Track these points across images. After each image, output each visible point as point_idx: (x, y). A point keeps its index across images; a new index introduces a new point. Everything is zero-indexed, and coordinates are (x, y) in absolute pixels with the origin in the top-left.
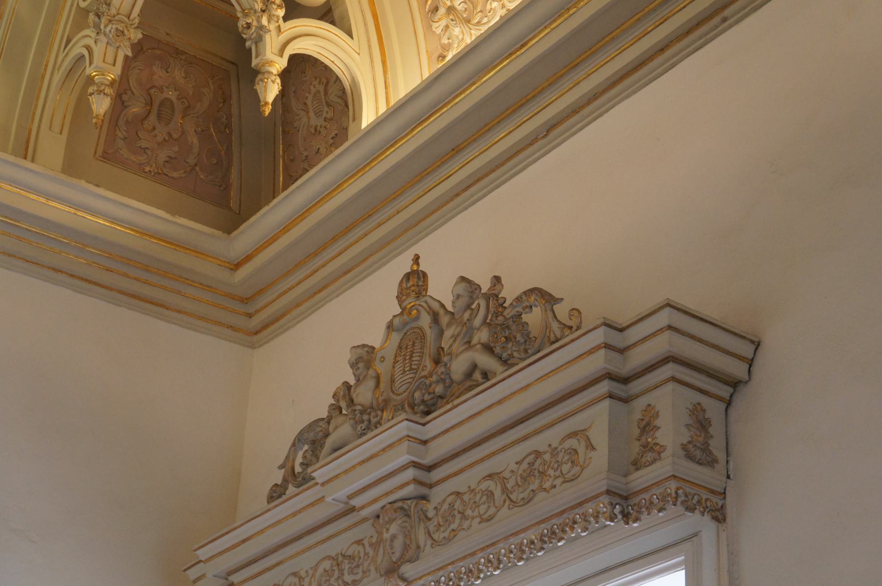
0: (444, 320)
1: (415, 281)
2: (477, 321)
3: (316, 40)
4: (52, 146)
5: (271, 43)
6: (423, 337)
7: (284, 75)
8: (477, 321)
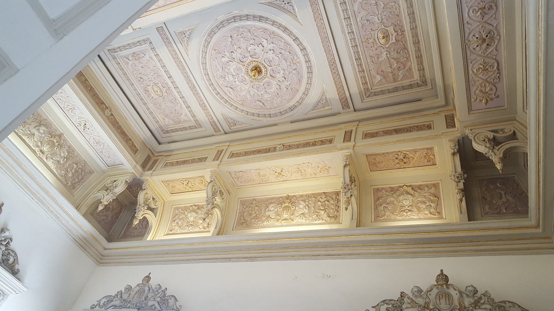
0: (151, 291)
1: (148, 278)
2: (158, 295)
3: (150, 216)
4: (84, 209)
5: (141, 213)
6: (144, 291)
7: (140, 220)
8: (158, 295)
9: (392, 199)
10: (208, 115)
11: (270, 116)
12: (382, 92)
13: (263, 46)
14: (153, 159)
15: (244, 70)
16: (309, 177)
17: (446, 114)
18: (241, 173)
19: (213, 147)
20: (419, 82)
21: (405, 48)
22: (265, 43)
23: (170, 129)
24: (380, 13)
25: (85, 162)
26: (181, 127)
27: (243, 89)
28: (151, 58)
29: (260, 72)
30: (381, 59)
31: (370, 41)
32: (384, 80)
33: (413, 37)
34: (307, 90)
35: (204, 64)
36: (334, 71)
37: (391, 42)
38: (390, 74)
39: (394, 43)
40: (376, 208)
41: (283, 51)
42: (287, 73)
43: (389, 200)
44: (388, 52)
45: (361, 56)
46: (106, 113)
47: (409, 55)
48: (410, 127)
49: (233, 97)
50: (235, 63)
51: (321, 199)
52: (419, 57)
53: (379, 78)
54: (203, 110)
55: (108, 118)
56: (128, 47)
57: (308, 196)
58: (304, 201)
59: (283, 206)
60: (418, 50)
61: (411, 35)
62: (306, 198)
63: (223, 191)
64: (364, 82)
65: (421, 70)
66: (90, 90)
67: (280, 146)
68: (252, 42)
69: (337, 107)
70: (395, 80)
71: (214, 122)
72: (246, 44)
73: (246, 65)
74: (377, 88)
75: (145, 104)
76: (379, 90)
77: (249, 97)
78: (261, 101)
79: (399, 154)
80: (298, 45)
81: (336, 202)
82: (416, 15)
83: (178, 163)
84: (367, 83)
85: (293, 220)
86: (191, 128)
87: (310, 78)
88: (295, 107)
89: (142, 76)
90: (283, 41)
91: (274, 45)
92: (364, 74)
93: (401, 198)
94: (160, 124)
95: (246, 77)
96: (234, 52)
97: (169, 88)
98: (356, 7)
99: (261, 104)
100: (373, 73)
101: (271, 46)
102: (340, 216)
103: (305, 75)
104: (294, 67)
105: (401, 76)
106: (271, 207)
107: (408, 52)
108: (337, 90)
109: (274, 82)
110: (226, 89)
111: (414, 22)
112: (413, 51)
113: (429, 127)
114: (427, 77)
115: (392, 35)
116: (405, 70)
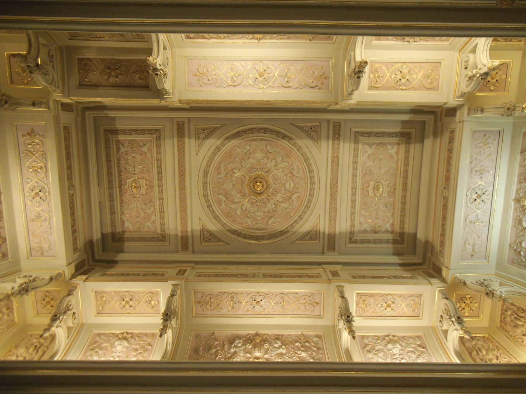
10: (336, 150)
13: (242, 209)
15: (271, 190)
18: (313, 85)
20: (111, 136)
22: (239, 212)
23: (398, 138)
25: (521, 153)
26: (381, 138)
27: (281, 170)
28: (361, 224)
30: (140, 167)
35: (307, 207)
41: (224, 199)
46: (447, 195)
50: (276, 200)
54: (338, 157)
55: (448, 189)
60: (109, 168)
61: (114, 183)
75: (405, 178)
76: (146, 135)
77: (279, 159)
86: (370, 134)
87: (208, 166)
90: (222, 207)
94: (406, 148)
95: (271, 181)
96: (271, 210)
98: (153, 217)
99: (269, 148)
101: (233, 206)
103: (212, 169)
104: (221, 180)
108: (184, 147)
112: (113, 168)
115: (128, 186)
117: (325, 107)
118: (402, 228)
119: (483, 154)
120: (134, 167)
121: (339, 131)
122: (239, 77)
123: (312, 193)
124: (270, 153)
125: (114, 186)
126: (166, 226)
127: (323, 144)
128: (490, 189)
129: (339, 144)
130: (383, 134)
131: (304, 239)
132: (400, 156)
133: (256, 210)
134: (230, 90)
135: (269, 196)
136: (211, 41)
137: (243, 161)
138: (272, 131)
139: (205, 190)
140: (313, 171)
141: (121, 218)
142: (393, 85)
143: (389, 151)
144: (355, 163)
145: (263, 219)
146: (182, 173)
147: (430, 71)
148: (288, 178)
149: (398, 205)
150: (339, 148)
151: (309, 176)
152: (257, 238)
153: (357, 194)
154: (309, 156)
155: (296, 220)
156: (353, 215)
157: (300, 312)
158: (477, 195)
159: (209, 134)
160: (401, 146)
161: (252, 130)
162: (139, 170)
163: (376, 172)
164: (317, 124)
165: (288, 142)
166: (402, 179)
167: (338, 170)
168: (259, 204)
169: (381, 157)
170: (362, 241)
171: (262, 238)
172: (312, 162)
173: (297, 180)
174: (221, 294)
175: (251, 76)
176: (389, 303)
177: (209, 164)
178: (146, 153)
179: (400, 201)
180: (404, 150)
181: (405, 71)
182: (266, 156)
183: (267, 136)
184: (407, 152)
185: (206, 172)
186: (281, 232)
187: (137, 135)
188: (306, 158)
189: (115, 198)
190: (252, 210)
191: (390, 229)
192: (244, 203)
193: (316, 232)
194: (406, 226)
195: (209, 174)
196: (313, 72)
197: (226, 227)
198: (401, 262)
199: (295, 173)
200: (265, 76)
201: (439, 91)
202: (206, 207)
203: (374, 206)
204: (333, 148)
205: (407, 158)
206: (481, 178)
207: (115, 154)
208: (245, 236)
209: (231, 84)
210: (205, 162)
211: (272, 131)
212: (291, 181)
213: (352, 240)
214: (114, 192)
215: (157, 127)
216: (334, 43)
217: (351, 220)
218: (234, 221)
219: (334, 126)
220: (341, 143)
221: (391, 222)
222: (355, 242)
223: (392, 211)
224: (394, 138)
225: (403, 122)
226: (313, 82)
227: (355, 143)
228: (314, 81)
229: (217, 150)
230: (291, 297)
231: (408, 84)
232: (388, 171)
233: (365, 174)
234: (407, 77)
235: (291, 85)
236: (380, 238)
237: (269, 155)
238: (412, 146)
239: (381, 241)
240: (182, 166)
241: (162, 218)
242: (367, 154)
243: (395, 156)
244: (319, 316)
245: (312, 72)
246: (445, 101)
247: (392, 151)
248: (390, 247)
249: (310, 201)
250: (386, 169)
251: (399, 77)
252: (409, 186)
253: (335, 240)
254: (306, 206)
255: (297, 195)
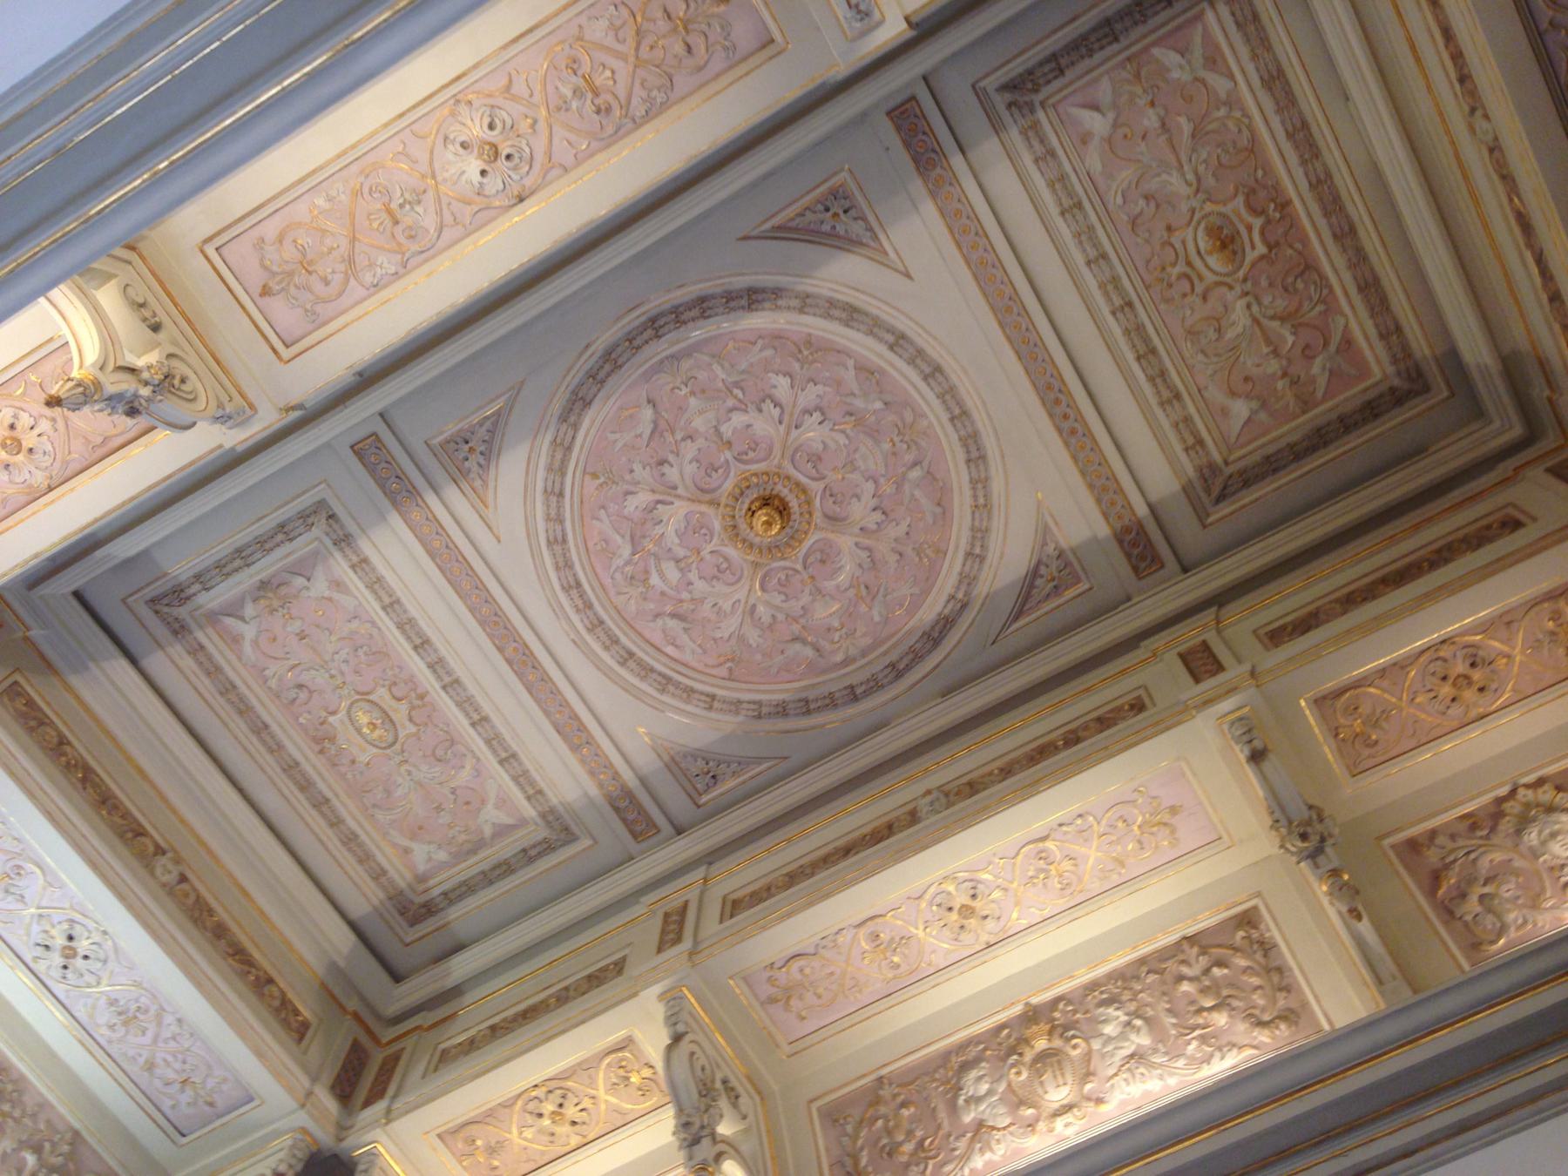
9: (1498, 856)
10: (597, 765)
11: (853, 695)
12: (1271, 465)
14: (377, 1057)
15: (717, 525)
16: (1097, 887)
17: (1549, 464)
18: (795, 966)
19: (638, 910)
20: (1396, 382)
21: (1308, 267)
23: (436, 892)
24: (1184, 159)
26: (485, 866)
27: (727, 606)
28: (338, 585)
29: (783, 510)
30: (1230, 334)
31: (1175, 271)
32: (1263, 416)
33: (1327, 214)
34: (980, 534)
35: (558, 542)
36: (1066, 425)
37: (1251, 256)
38: (1280, 384)
39: (1262, 257)
40: (1448, 912)
41: (859, 403)
42: (888, 488)
43: (1484, 864)
44: (1249, 298)
45: (1156, 341)
46: (158, 871)
47: (1331, 290)
48: (1439, 551)
49: (688, 657)
50: (677, 503)
51: (1185, 970)
52: (1370, 287)
53: (1241, 409)
54: (575, 749)
56: (238, 563)
57: (1126, 977)
58: (1111, 1001)
59: (1029, 1056)
60: (1359, 259)
62: (1118, 988)
63: (734, 1082)
64: (1191, 440)
65: (1391, 332)
66: (84, 780)
67: (928, 799)
68: (730, 403)
69: (1113, 569)
70: (1306, 404)
71: (628, 794)
72: (711, 415)
73: (723, 501)
74: (1249, 454)
76: (1256, 457)
77: (753, 636)
78: (804, 642)
79: (1445, 652)
80: (911, 362)
81: (1259, 956)
82: (1314, 129)
83: (495, 1032)
84: (1201, 442)
85: (1099, 1101)
86: (528, 856)
87: (980, 484)
88: (945, 624)
89: (305, 678)
90: (851, 363)
91: (820, 389)
92: (1184, 407)
93: (1532, 837)
94: (391, 881)
95: (732, 552)
96: (671, 458)
97: (421, 697)
98: (1094, 161)
99: (809, 652)
100: (1216, 395)
101: (810, 396)
102: (1305, 1005)
103: (958, 475)
104: (909, 458)
105: (1322, 382)
106: (976, 1083)
107: (1322, 277)
108: (1099, 501)
109: (845, 542)
110: (654, 631)
111: (1317, 155)
113: (1512, 525)
114: (1418, 355)
116: (1332, 348)
117: (713, 868)
118: (197, 650)
119: (170, 1059)
120: (1256, 321)
121: (624, 820)
122: (1031, 873)
123: (574, 592)
124: (795, 639)
125: (1308, 196)
126: (1027, 159)
127: (647, 761)
128: (60, 989)
129: (601, 785)
130: (488, 878)
131: (488, 424)
132: (388, 850)
133: (723, 429)
134: (1038, 827)
135: (711, 503)
136: (1175, 937)
137: (867, 563)
138: (831, 702)
139: (949, 395)
140: (623, 664)
141: (1232, 77)
142: (570, 1084)
143: (432, 848)
144: (508, 759)
145: (681, 409)
146: (1058, 410)
147: (496, 1163)
148: (685, 595)
149: (270, 712)
150: (592, 773)
151: (623, 639)
152: (655, 326)
153: (428, 672)
154: (665, 698)
155: (563, 475)
156: (387, 600)
157: (301, 211)
158: (81, 952)
159: (1032, 586)
160: (409, 876)
161: (897, 671)
162: (1233, 317)
163: (424, 768)
164: (704, 799)
165: (759, 703)
166: (329, 795)
167: (547, 713)
168: (728, 455)
169: (445, 818)
170: (284, 532)
171: (633, 341)
172: (644, 686)
173: (652, 606)
174: (660, 98)
175: (997, 894)
176: (20, 457)
177: (980, 493)
178: (1233, 394)
179: (274, 727)
180: (392, 873)
181: (563, 1129)
182: (802, 621)
183: (835, 682)
184: (379, 875)
185: (976, 457)
186: (587, 404)
187: (1294, 438)
188: (671, 688)
189: (1287, 147)
190: (738, 419)
191: (229, 621)
192: (782, 428)
193: (465, 474)
194: (188, 662)
195: (961, 456)
196: (819, 997)
197: (795, 303)
198: (99, 553)
199: (672, 623)
200: (954, 916)
201: (433, 1134)
202: (909, 333)
203: (344, 667)
204: (609, 765)
205: (365, 858)
206: (113, 1002)
207: (1353, 325)
208: (702, 307)
209: (1050, 845)
210: (997, 485)
211: (831, 702)
212: (672, 593)
213: (324, 515)
214: (1299, 173)
215: (1226, 509)
216: (811, 1101)
217: (380, 580)
218: (776, 338)
219: (652, 824)
220: (594, 791)
221: (247, 648)
222: (304, 519)
223: (273, 683)
224: (447, 886)
225: (459, 948)
226: (801, 970)
227: (552, 811)
228: (798, 976)
229: (977, 551)
230: (382, 259)
231: (531, 1106)
232: (388, 792)
233: (453, 742)
234: (546, 1122)
235: (863, 933)
236: (237, 577)
237: (796, 628)
238: (376, 895)
239: (223, 568)
240: (1073, 432)
241: (1059, 182)
242: (492, 801)
243: (406, 842)
244: (215, 243)
245: (821, 990)
246: (396, 1126)
247: (423, 855)
248: (180, 568)
249: (564, 565)
250: (399, 792)
251: (571, 1112)
252: (290, 788)
253: (382, 487)
254: (564, 541)
255: (620, 562)
